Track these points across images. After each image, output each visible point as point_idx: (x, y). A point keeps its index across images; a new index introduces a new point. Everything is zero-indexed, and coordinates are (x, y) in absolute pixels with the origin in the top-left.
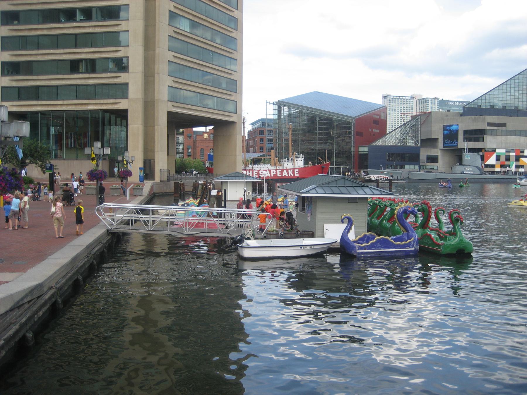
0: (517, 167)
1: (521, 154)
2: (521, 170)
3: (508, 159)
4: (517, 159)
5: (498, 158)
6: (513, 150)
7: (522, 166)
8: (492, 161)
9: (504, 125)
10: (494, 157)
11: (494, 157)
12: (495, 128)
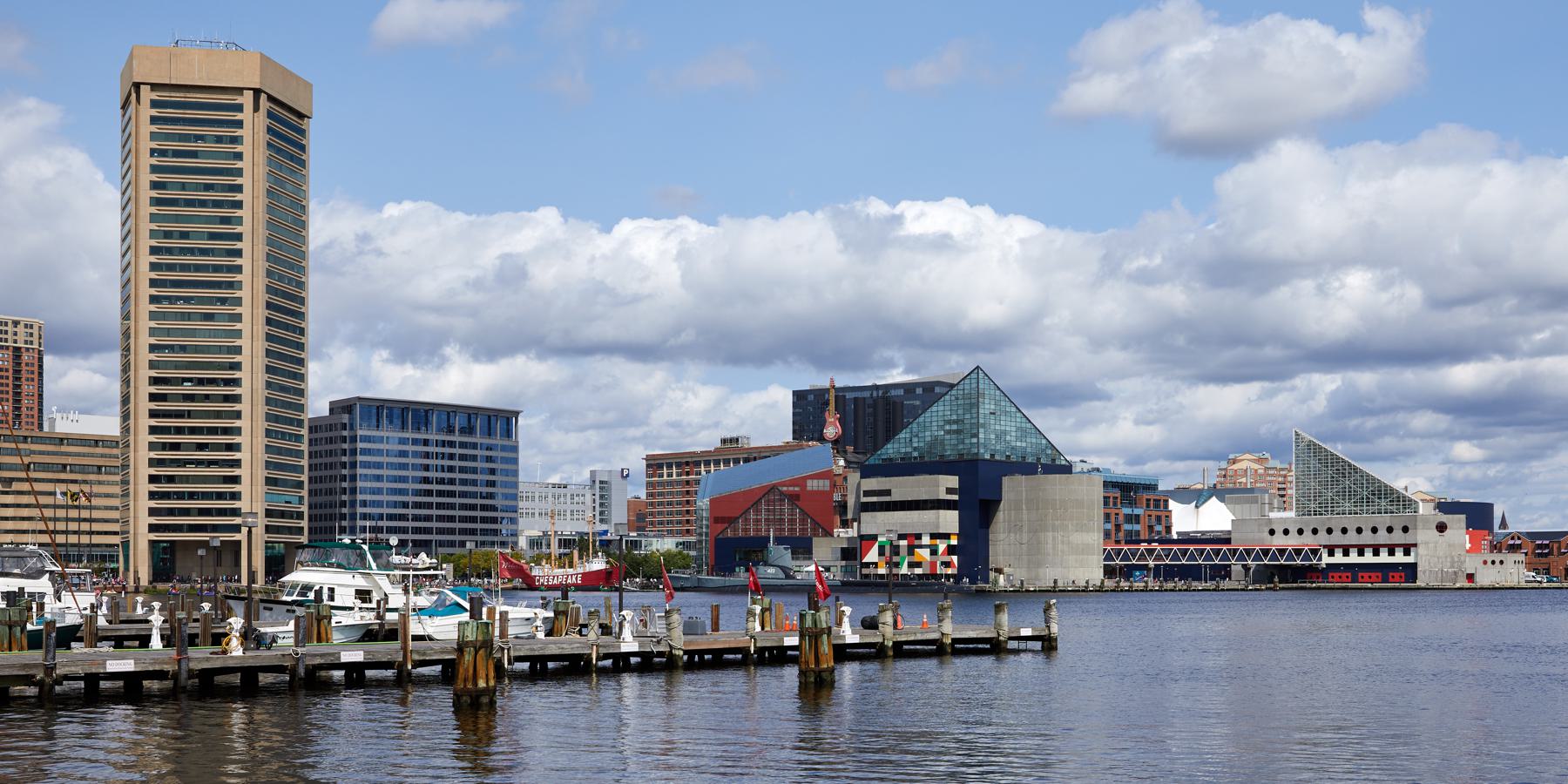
0: (911, 565)
1: (917, 542)
2: (918, 571)
3: (896, 550)
4: (911, 550)
5: (881, 552)
6: (901, 537)
7: (919, 565)
8: (872, 556)
9: (888, 493)
10: (875, 549)
11: (875, 549)
12: (875, 499)
